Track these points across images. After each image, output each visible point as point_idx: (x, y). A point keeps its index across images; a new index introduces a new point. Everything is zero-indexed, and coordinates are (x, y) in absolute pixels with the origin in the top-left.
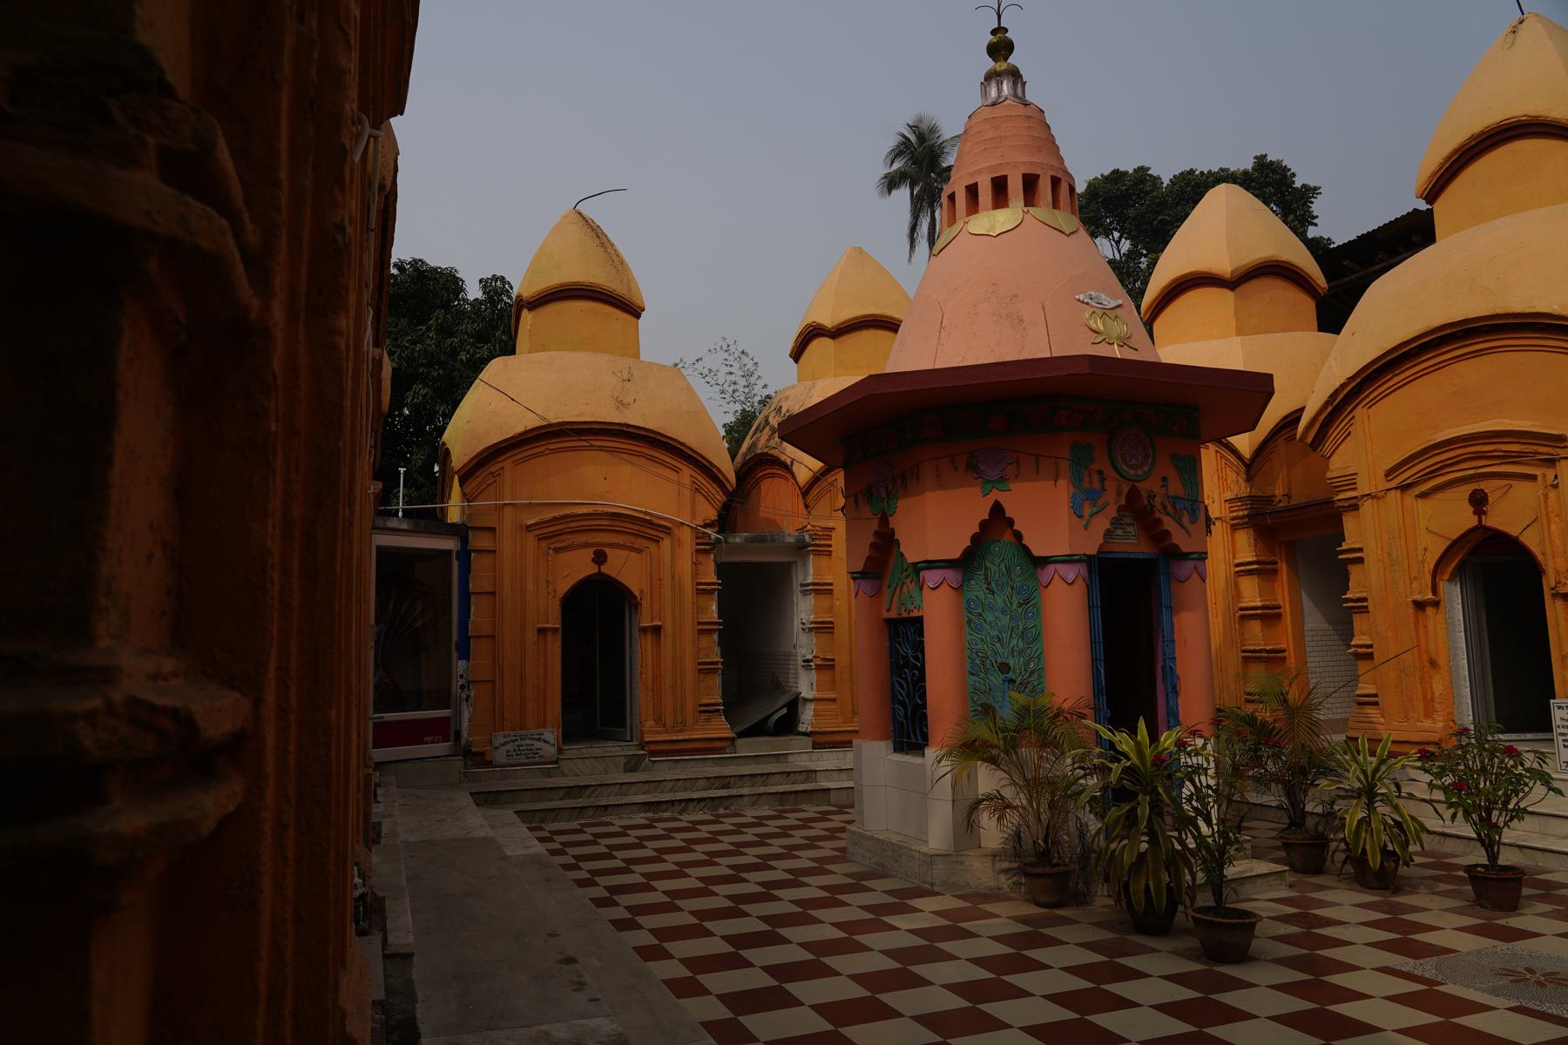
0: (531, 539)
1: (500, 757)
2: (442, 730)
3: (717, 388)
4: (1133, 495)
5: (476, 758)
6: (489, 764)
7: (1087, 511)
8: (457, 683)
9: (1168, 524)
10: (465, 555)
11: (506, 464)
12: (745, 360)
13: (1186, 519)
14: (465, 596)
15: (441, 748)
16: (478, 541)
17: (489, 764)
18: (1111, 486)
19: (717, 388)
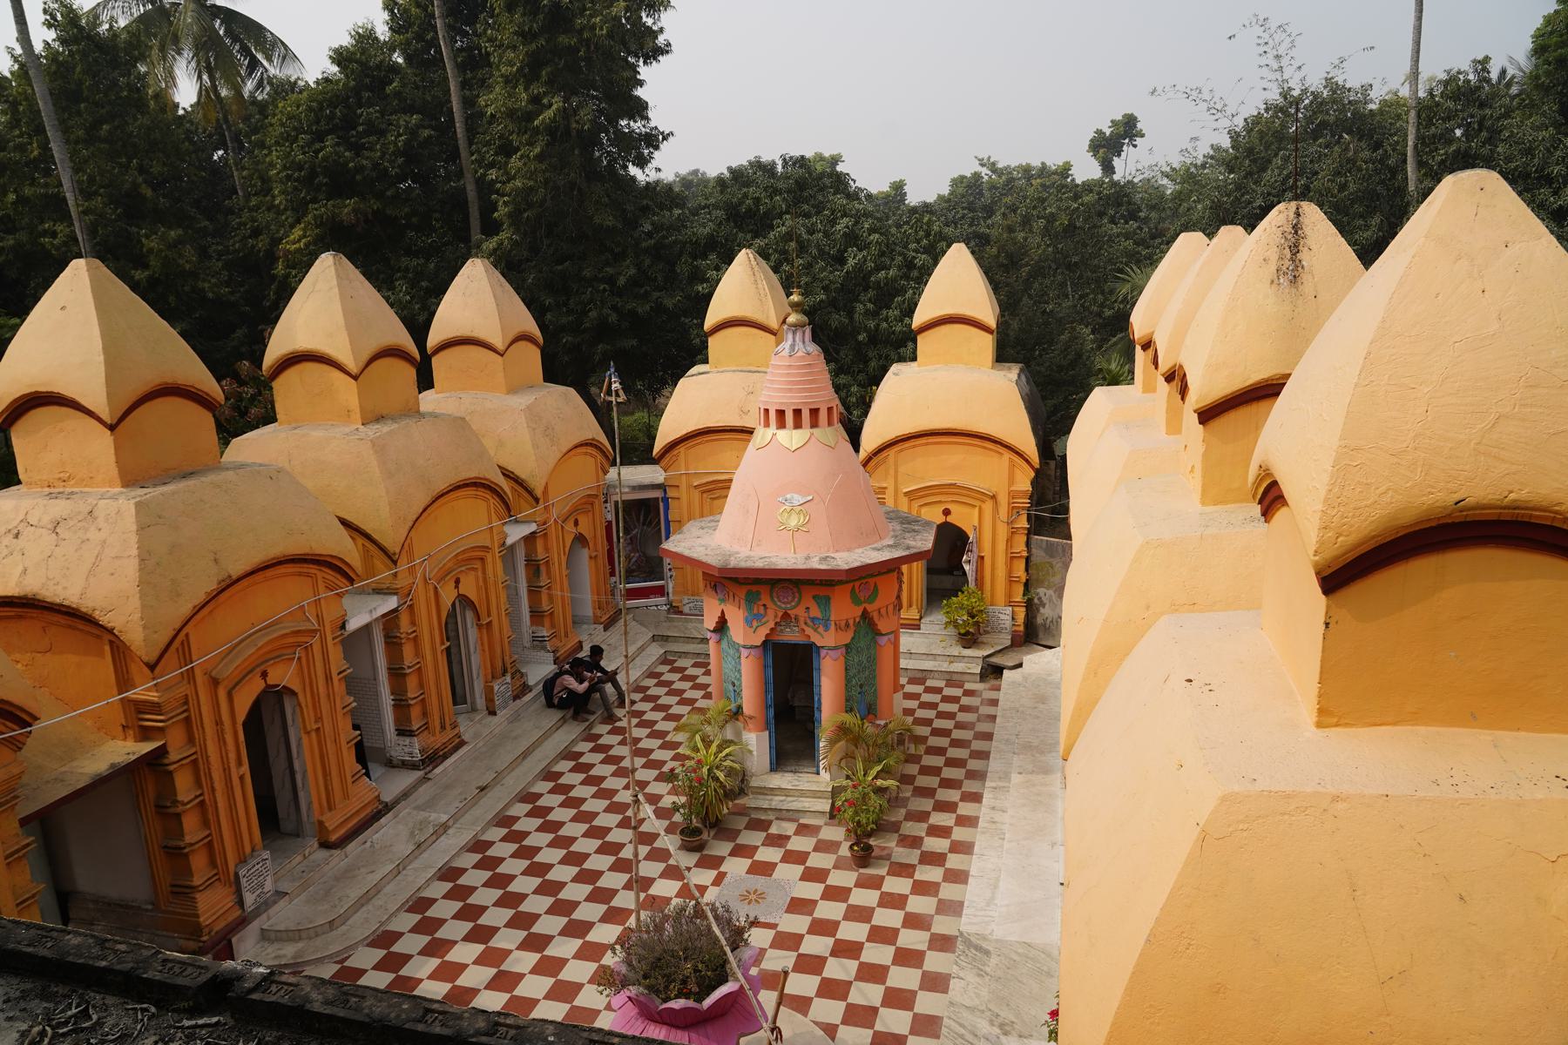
0: (696, 494)
1: (686, 609)
2: (660, 591)
3: (1205, 105)
4: (786, 616)
5: (675, 609)
6: (681, 613)
7: (755, 624)
8: (666, 567)
9: (809, 631)
10: (665, 500)
11: (681, 449)
12: (1279, 36)
13: (821, 629)
14: (668, 522)
15: (662, 600)
16: (671, 493)
17: (681, 613)
18: (771, 613)
19: (1205, 105)
